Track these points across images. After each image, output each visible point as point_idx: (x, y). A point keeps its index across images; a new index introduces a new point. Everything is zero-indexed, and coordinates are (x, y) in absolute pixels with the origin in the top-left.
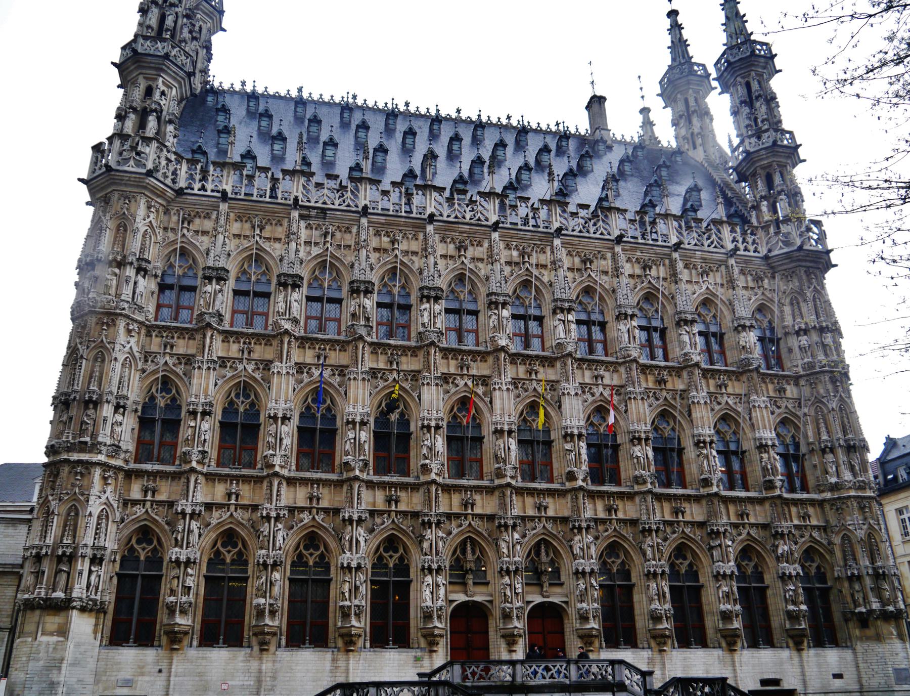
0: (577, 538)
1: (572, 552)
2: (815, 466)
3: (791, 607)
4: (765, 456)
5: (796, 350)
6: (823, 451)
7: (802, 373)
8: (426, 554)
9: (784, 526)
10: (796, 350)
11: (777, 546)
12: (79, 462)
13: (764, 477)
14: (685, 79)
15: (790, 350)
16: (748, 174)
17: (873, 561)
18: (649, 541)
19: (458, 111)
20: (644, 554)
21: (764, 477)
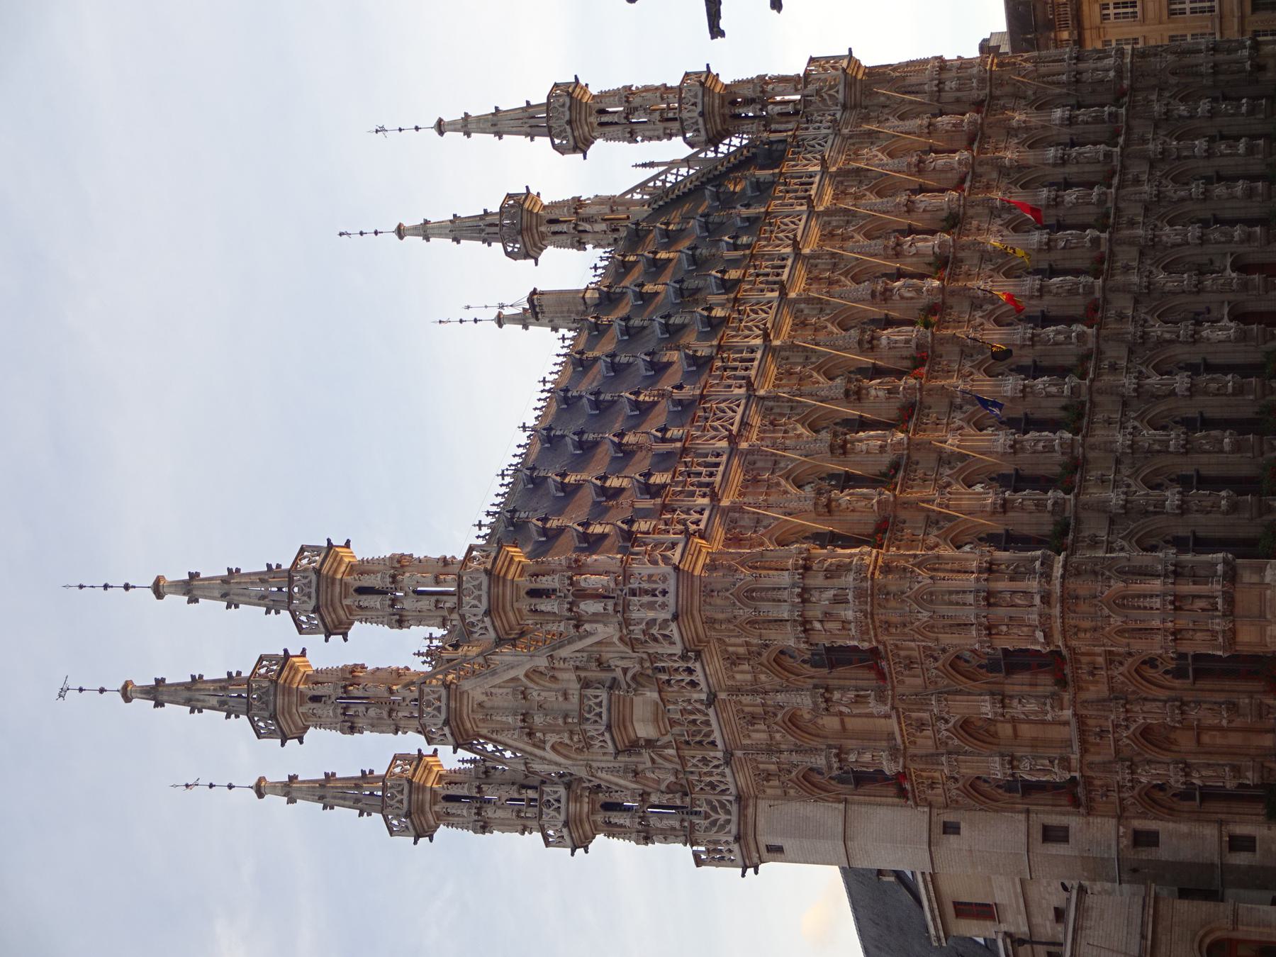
0: (1164, 238)
1: (1179, 245)
2: (1093, 91)
3: (1244, 109)
4: (1080, 118)
5: (959, 94)
6: (1078, 81)
7: (987, 91)
8: (1178, 336)
9: (1157, 108)
10: (959, 94)
11: (1180, 116)
12: (1064, 567)
13: (1103, 122)
14: (525, 214)
15: (958, 100)
16: (719, 128)
17: (1200, 51)
18: (1171, 193)
19: (524, 428)
20: (1182, 200)
21: (1103, 122)
